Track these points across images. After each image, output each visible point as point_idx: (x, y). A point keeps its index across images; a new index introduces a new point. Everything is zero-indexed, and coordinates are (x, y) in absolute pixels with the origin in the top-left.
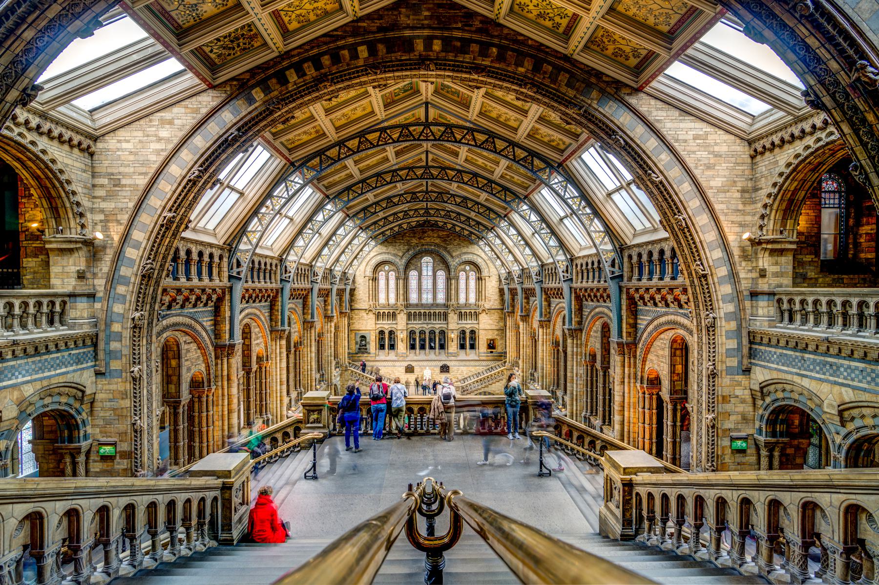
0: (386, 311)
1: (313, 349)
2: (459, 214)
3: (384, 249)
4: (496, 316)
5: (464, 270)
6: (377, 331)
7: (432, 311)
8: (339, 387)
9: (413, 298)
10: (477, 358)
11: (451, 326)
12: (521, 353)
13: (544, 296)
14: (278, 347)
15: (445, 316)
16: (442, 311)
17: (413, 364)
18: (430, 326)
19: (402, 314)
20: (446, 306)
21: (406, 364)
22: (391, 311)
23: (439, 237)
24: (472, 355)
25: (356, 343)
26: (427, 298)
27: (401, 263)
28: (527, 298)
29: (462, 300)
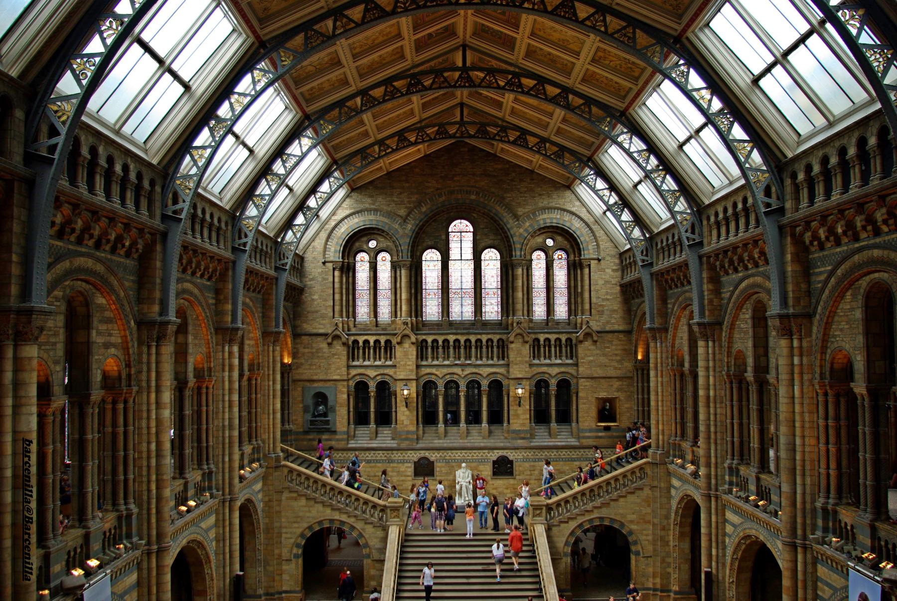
0: (372, 340)
1: (167, 396)
2: (542, 80)
3: (367, 203)
4: (615, 346)
5: (544, 249)
6: (352, 383)
7: (473, 339)
8: (260, 506)
9: (432, 309)
10: (573, 442)
11: (517, 371)
12: (702, 417)
13: (789, 249)
14: (9, 366)
15: (503, 346)
16: (496, 338)
17: (433, 456)
18: (468, 371)
19: (407, 345)
20: (501, 326)
21: (415, 456)
22: (383, 340)
24: (563, 437)
25: (306, 410)
26: (461, 310)
27: (404, 232)
28: (715, 280)
29: (539, 311)
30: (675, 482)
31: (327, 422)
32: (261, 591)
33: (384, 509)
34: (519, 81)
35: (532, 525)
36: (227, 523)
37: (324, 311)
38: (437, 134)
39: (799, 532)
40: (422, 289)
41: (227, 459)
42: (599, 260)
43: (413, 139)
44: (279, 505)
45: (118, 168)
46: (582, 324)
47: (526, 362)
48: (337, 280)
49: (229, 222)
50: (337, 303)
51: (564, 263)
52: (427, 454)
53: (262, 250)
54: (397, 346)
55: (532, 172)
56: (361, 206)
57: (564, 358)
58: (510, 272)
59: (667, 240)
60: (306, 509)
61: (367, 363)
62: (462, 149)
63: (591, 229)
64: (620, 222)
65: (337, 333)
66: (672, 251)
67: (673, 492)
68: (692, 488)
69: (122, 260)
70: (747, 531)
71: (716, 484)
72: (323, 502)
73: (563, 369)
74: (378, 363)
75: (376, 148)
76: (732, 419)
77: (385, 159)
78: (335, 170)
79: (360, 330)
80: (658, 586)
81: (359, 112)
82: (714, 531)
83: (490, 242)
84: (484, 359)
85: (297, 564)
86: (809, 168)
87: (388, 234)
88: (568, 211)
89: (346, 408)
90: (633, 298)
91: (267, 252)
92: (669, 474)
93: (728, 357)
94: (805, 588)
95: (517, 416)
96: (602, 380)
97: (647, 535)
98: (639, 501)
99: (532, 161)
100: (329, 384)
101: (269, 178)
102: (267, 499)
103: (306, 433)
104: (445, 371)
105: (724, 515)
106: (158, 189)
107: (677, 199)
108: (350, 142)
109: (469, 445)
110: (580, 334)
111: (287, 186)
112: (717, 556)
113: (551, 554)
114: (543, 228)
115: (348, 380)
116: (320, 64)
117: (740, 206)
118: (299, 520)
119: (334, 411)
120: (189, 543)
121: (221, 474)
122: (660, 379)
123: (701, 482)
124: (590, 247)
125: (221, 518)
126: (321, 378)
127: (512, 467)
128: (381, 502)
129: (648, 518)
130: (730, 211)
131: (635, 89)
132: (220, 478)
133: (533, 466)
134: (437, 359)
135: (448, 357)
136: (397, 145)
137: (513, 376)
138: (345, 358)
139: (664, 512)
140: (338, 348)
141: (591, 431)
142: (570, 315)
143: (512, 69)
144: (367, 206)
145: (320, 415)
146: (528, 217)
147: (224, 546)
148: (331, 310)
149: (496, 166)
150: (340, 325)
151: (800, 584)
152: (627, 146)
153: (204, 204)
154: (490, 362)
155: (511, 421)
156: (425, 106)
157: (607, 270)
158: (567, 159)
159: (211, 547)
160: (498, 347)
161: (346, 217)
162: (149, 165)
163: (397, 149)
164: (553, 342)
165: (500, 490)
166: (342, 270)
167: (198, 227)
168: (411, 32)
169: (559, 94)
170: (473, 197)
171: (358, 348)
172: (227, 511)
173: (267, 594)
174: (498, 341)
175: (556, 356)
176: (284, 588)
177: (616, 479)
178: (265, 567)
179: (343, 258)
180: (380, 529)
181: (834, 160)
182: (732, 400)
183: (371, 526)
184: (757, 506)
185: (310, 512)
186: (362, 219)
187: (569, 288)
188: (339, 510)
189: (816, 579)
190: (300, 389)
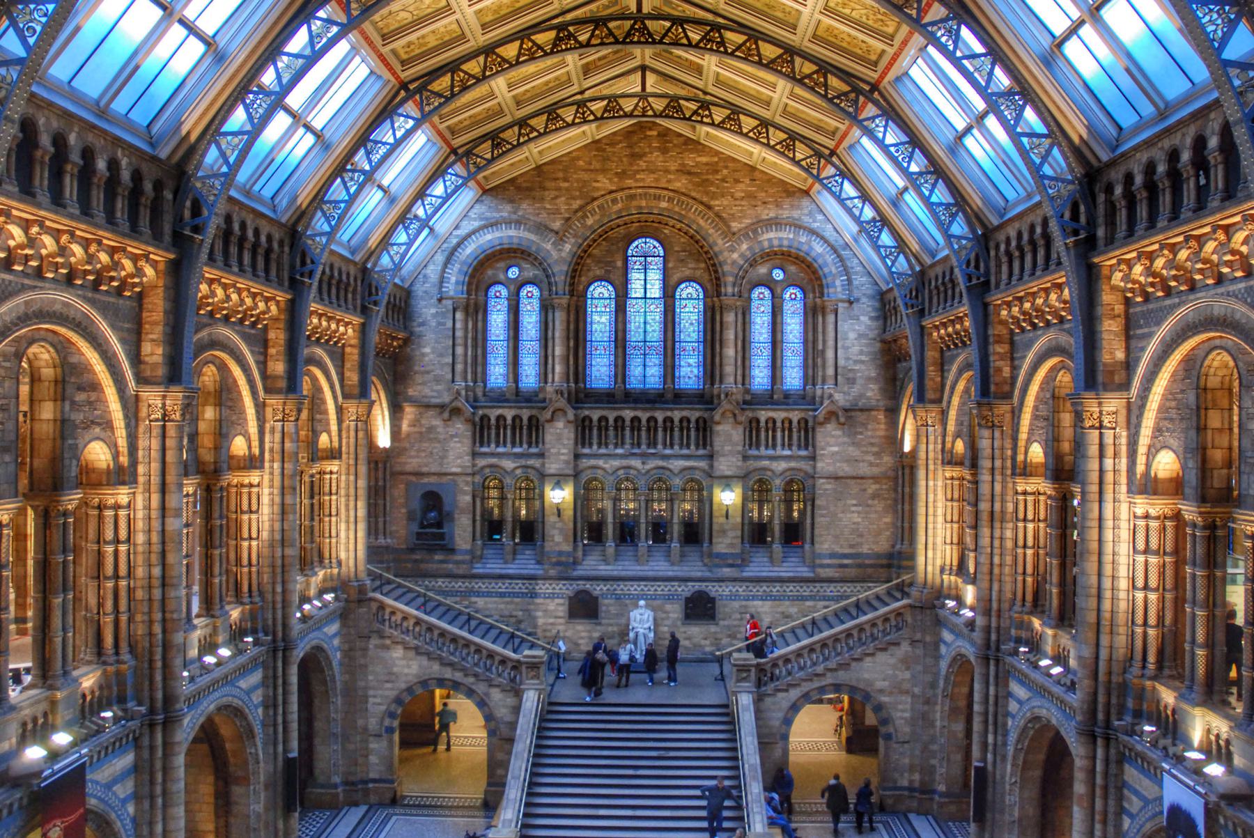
0: (509, 414)
2: (755, 36)
3: (505, 211)
5: (769, 283)
6: (478, 479)
10: (804, 572)
11: (725, 465)
15: (704, 430)
16: (694, 415)
17: (598, 589)
18: (652, 464)
19: (560, 424)
20: (705, 399)
22: (525, 414)
23: (684, 171)
25: (410, 517)
27: (559, 254)
29: (760, 376)
30: (947, 636)
31: (441, 536)
32: (337, 779)
33: (517, 666)
34: (721, 36)
35: (735, 693)
36: (280, 681)
37: (438, 372)
38: (605, 110)
39: (1100, 716)
40: (585, 340)
41: (279, 589)
42: (851, 303)
43: (569, 119)
44: (364, 656)
45: (101, 165)
46: (822, 397)
47: (739, 452)
48: (459, 325)
49: (287, 242)
50: (460, 359)
51: (799, 305)
53: (340, 281)
54: (547, 426)
55: (753, 169)
57: (794, 448)
58: (718, 318)
59: (944, 277)
60: (404, 662)
61: (501, 450)
62: (649, 133)
63: (839, 256)
64: (877, 248)
65: (459, 405)
66: (950, 292)
67: (943, 649)
68: (968, 646)
69: (112, 300)
70: (1036, 710)
71: (998, 641)
72: (428, 655)
73: (793, 464)
74: (517, 450)
75: (516, 129)
77: (532, 145)
78: (454, 163)
79: (493, 400)
80: (917, 785)
81: (481, 79)
82: (991, 709)
83: (688, 273)
84: (676, 447)
85: (391, 742)
86: (1129, 178)
87: (536, 259)
88: (805, 228)
89: (471, 516)
90: (900, 361)
91: (348, 284)
92: (939, 622)
96: (853, 482)
97: (903, 711)
98: (893, 661)
99: (751, 154)
100: (445, 479)
101: (345, 175)
102: (346, 647)
103: (412, 550)
104: (616, 463)
105: (1007, 685)
106: (168, 195)
107: (953, 216)
108: (476, 122)
109: (651, 574)
110: (821, 413)
111: (380, 187)
112: (995, 745)
113: (759, 736)
114: (768, 254)
115: (473, 474)
116: (417, 9)
117: (1039, 230)
118: (393, 678)
119: (452, 520)
120: (219, 709)
121: (270, 611)
122: (931, 483)
123: (978, 636)
124: (838, 283)
125: (271, 673)
126: (433, 470)
127: (713, 608)
128: (512, 655)
129: (906, 686)
130: (1026, 237)
131: (891, 51)
132: (270, 616)
133: (746, 607)
134: (607, 445)
135: (623, 443)
136: (546, 127)
137: (717, 473)
138: (468, 442)
139: (929, 678)
140: (460, 427)
141: (833, 555)
142: (805, 385)
143: (710, 17)
144: (505, 214)
145: (431, 526)
146: (746, 235)
147: (275, 714)
148: (449, 369)
149: (699, 159)
150: (463, 393)
151: (1098, 792)
152: (880, 136)
153: (244, 214)
154: (685, 451)
155: (714, 540)
156: (587, 70)
157: (862, 318)
158: (801, 152)
159: (257, 715)
160: (697, 429)
161: (474, 232)
162: (154, 159)
163: (545, 133)
165: (695, 640)
166: (466, 310)
167: (234, 250)
169: (780, 56)
170: (664, 205)
171: (489, 428)
172: (280, 664)
173: (346, 783)
174: (697, 421)
175: (783, 445)
176: (372, 775)
177: (861, 628)
178: (343, 745)
179: (469, 293)
180: (512, 694)
181: (1161, 168)
184: (1050, 676)
185: (409, 667)
186: (497, 234)
187: (805, 342)
188: (451, 665)
189: (1122, 785)
190: (402, 486)
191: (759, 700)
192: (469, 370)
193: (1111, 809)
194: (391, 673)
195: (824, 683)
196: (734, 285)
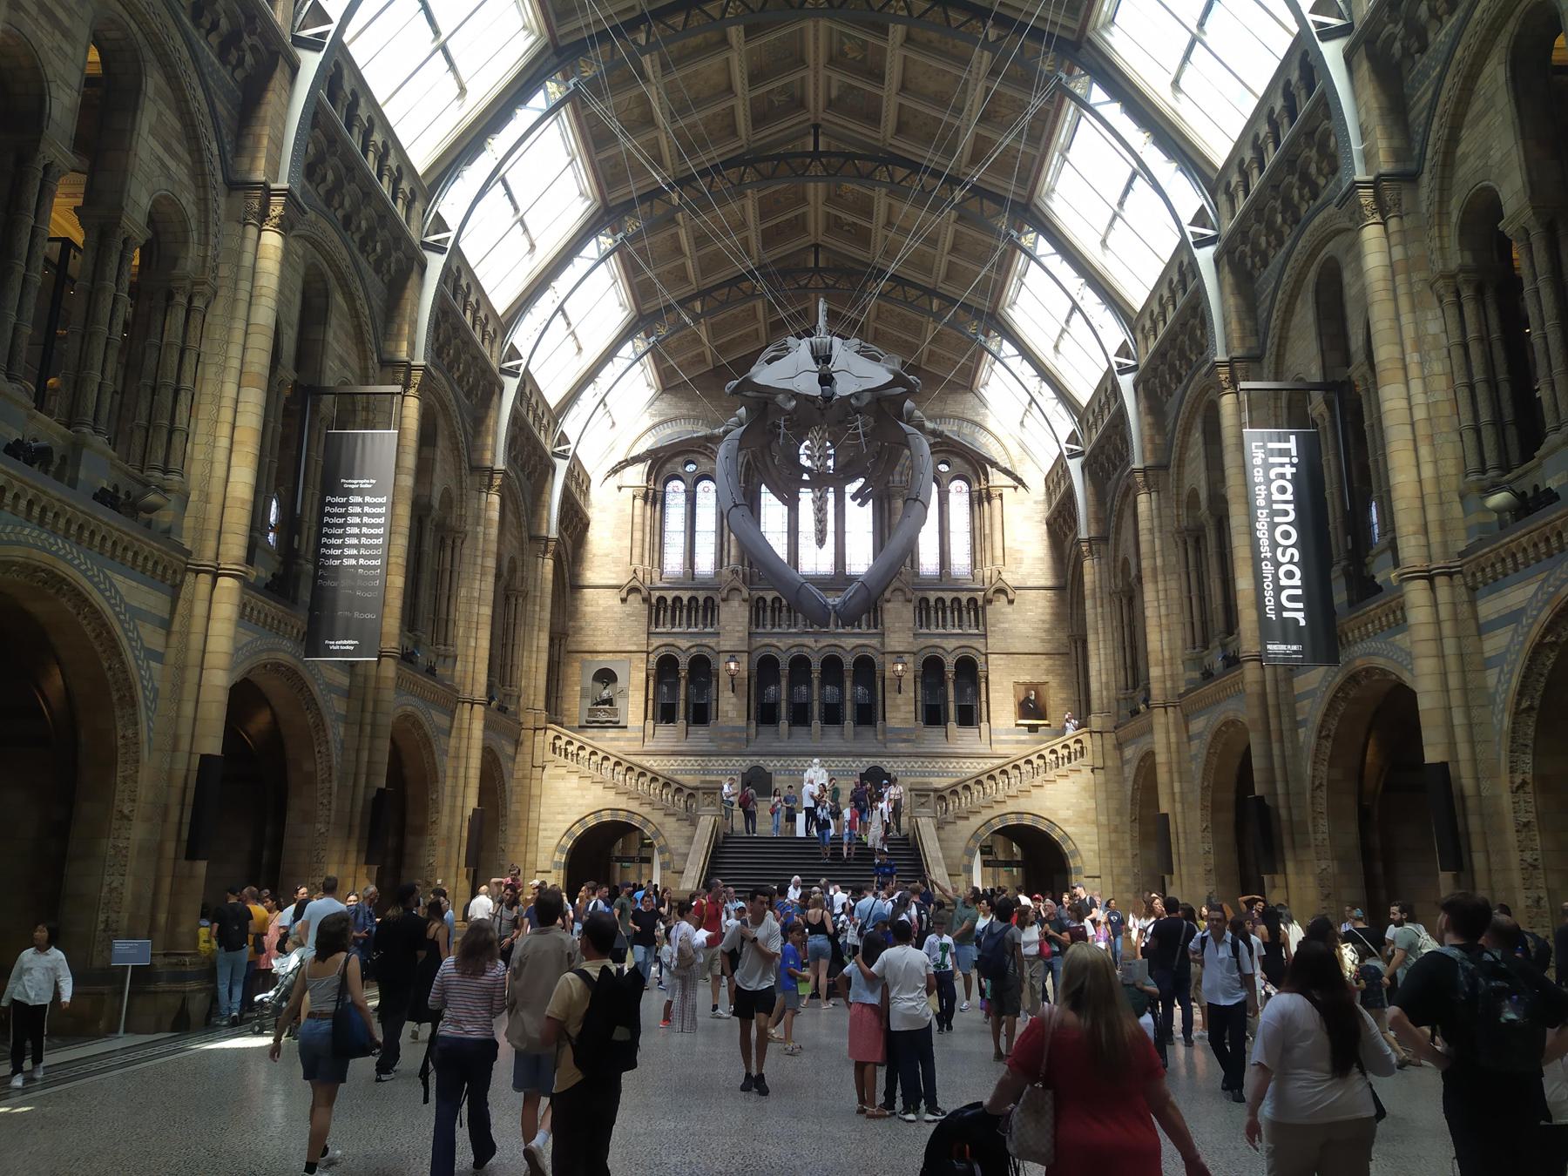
0: (685, 596)
3: (684, 408)
6: (653, 658)
17: (771, 764)
19: (735, 603)
21: (743, 764)
22: (701, 596)
29: (928, 561)
47: (909, 629)
50: (638, 543)
52: (761, 762)
54: (721, 604)
56: (676, 412)
58: (886, 506)
60: (579, 793)
75: (698, 306)
76: (1190, 592)
93: (1178, 507)
94: (1279, 716)
95: (897, 707)
104: (791, 641)
118: (565, 808)
141: (1008, 732)
144: (684, 412)
151: (1272, 712)
164: (948, 603)
166: (645, 498)
168: (747, 87)
182: (1187, 567)
183: (673, 819)
185: (583, 797)
186: (677, 429)
191: (939, 828)
192: (647, 555)
193: (1286, 726)
194: (566, 805)
195: (1005, 811)
196: (901, 474)
